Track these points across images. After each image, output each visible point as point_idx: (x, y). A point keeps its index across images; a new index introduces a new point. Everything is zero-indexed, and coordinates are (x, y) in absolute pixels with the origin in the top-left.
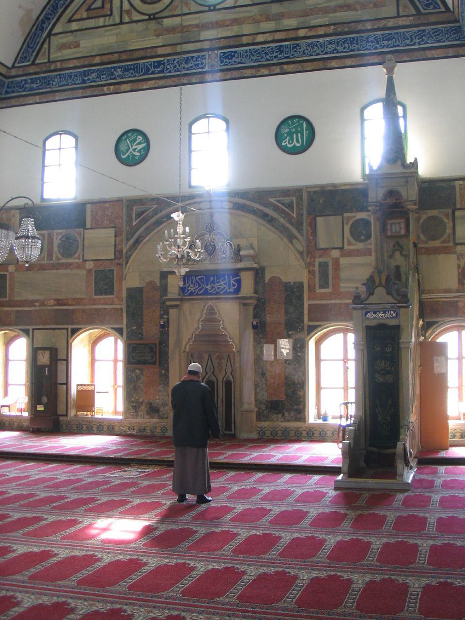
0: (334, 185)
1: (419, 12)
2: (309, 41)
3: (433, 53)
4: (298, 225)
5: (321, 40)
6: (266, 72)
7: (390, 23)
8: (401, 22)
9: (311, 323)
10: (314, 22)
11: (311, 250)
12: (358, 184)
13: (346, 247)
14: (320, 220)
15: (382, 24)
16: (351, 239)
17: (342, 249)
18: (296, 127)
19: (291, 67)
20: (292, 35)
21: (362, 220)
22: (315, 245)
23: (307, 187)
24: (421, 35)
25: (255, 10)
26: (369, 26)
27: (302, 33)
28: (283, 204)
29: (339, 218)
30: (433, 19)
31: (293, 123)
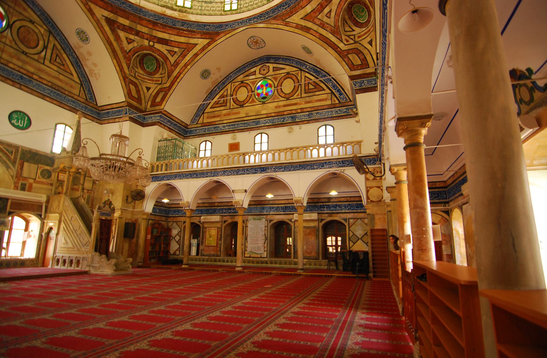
0: (37, 151)
1: (87, 100)
2: (38, 83)
3: (89, 117)
4: (14, 163)
5: (44, 86)
6: (11, 84)
7: (75, 97)
8: (80, 99)
9: (12, 210)
10: (42, 76)
11: (19, 176)
12: (48, 154)
13: (37, 179)
14: (26, 164)
15: (72, 95)
16: (40, 176)
17: (35, 179)
18: (22, 118)
19: (25, 89)
20: (30, 75)
21: (47, 170)
22: (21, 174)
23: (22, 147)
24: (86, 108)
25: (11, 50)
26: (67, 93)
27: (35, 77)
28: (7, 150)
29: (37, 166)
30: (91, 105)
31: (20, 115)
